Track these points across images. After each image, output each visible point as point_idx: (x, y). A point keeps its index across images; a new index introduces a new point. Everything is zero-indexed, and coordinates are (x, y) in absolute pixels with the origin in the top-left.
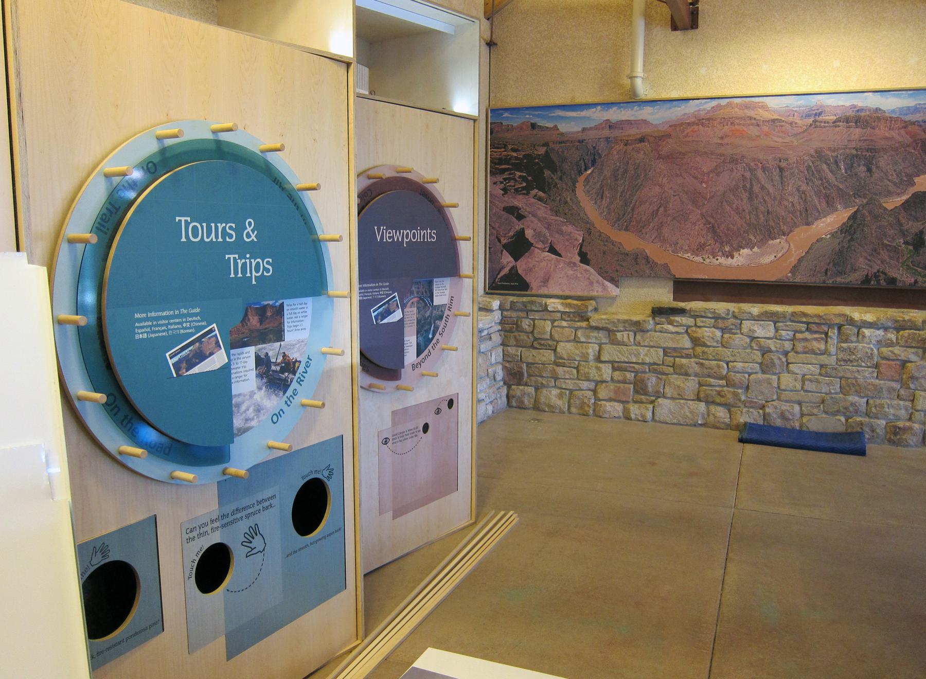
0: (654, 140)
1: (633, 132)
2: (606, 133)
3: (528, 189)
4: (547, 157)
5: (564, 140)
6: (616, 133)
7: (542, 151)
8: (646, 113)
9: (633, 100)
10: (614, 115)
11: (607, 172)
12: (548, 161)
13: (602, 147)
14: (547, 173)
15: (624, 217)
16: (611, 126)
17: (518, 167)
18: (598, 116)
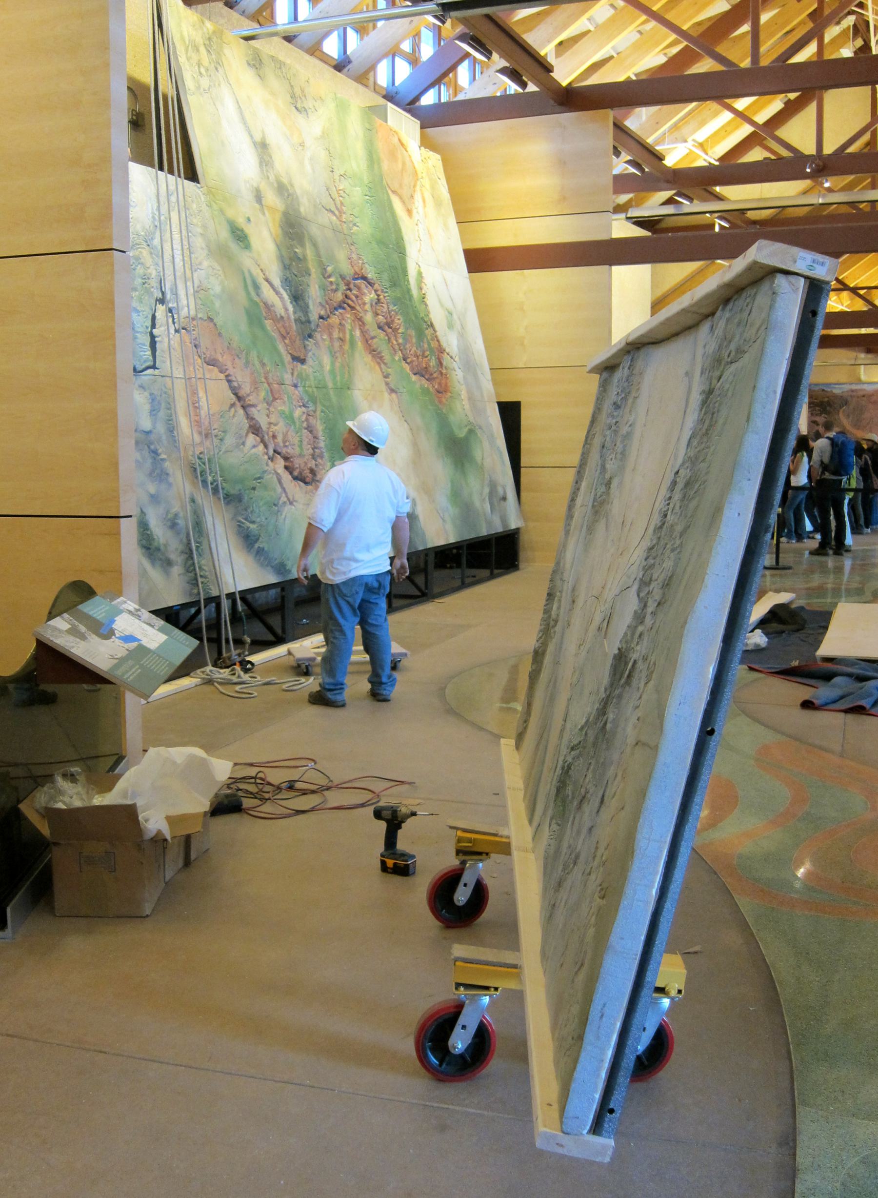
0: (867, 396)
1: (861, 393)
2: (850, 393)
3: (821, 414)
4: (828, 402)
5: (835, 396)
6: (854, 394)
7: (826, 400)
8: (865, 387)
9: (860, 382)
10: (854, 387)
11: (851, 407)
12: (829, 403)
13: (849, 399)
14: (828, 408)
15: (857, 425)
16: (852, 391)
17: (817, 405)
18: (847, 388)
